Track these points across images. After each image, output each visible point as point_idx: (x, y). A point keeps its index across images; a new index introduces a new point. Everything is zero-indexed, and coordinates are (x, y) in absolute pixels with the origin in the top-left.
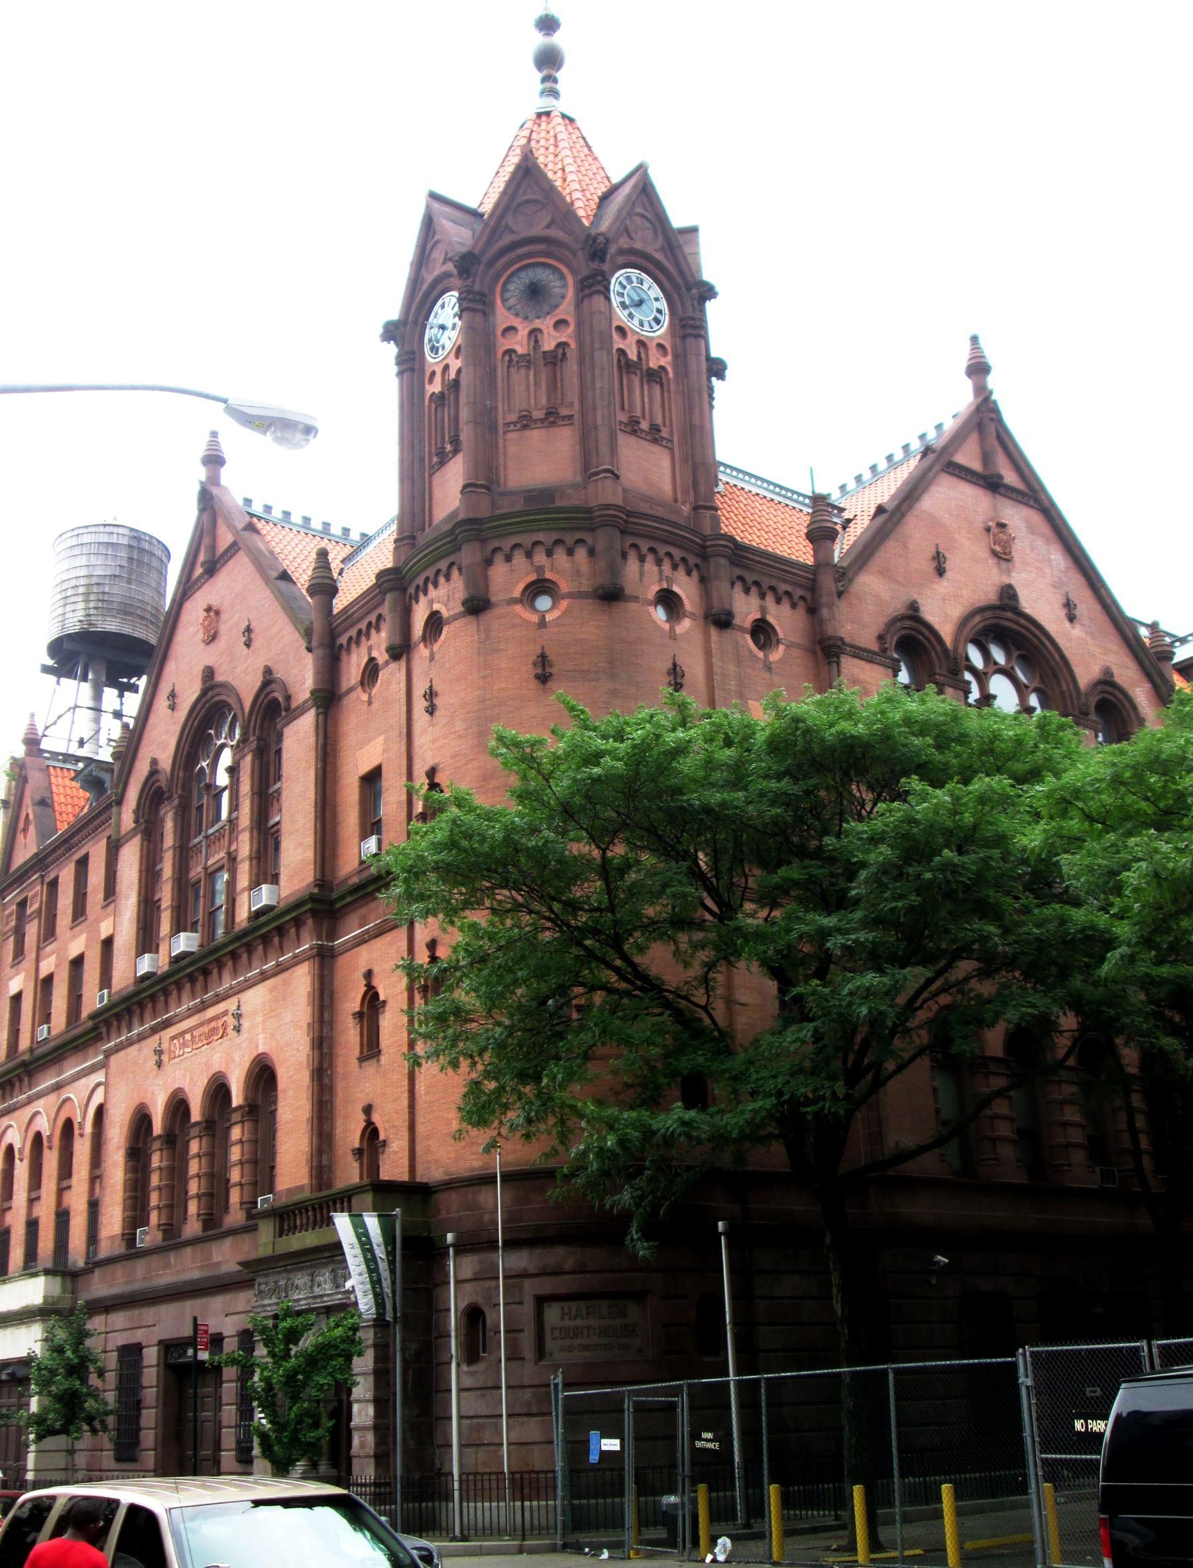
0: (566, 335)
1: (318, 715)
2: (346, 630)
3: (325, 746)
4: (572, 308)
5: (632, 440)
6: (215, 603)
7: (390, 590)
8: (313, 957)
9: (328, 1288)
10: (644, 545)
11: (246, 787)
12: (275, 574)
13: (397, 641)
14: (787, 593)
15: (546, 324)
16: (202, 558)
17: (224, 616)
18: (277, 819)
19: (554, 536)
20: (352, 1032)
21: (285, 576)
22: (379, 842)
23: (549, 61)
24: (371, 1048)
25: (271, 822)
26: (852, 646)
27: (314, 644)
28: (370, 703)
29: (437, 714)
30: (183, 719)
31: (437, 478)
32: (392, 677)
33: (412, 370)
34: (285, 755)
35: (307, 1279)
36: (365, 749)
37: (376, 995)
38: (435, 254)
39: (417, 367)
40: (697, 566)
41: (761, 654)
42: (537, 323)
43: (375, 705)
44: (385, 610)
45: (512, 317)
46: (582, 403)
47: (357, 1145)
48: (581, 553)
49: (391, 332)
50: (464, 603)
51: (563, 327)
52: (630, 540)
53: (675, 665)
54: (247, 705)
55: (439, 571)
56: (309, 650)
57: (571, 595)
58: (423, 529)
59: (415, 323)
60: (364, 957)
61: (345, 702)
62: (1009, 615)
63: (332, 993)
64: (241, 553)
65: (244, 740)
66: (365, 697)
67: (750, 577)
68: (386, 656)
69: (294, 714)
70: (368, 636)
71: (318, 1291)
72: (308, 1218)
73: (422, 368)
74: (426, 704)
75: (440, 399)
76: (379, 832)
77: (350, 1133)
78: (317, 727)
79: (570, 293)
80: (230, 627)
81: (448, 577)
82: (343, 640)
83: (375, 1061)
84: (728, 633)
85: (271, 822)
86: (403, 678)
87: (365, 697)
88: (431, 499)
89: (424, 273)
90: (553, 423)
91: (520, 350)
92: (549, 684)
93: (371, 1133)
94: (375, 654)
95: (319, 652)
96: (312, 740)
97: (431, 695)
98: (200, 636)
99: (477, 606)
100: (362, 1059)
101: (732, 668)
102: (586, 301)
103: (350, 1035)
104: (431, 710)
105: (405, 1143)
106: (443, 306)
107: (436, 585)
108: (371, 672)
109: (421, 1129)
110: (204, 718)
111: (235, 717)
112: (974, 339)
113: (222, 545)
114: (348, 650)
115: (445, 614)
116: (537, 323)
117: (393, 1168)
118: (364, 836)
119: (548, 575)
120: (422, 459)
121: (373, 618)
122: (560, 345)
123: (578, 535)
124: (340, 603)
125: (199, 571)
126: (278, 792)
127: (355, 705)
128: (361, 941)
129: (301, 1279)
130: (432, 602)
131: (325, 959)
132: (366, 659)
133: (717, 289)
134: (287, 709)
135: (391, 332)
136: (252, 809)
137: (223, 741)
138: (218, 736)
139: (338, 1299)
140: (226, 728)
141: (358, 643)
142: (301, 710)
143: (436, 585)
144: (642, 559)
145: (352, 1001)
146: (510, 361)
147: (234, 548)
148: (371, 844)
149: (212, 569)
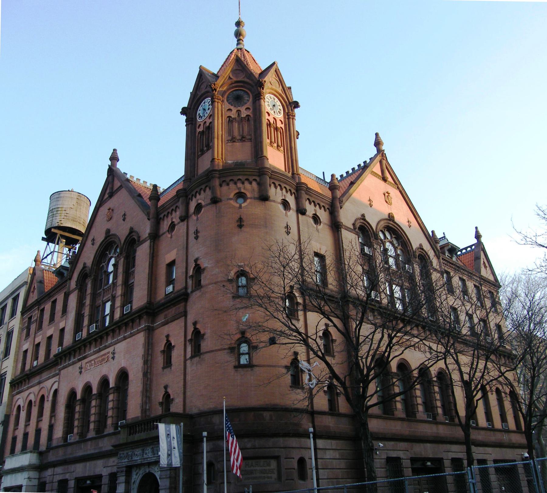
0: (249, 113)
1: (151, 242)
2: (163, 212)
3: (153, 253)
4: (252, 104)
5: (271, 148)
6: (112, 207)
7: (182, 196)
8: (145, 330)
9: (150, 455)
10: (277, 183)
11: (120, 270)
12: (136, 195)
13: (183, 214)
14: (323, 206)
15: (243, 109)
16: (108, 191)
17: (115, 211)
18: (133, 281)
19: (246, 177)
20: (160, 358)
21: (140, 195)
22: (174, 287)
23: (238, 35)
24: (168, 363)
25: (130, 283)
26: (345, 226)
27: (151, 217)
28: (171, 237)
29: (199, 239)
30: (97, 248)
31: (200, 159)
32: (181, 228)
33: (192, 124)
34: (137, 258)
35: (140, 452)
36: (169, 254)
37: (171, 344)
38: (202, 86)
39: (194, 123)
40: (294, 193)
41: (315, 226)
42: (239, 108)
43: (174, 238)
44: (179, 204)
45: (230, 106)
46: (255, 135)
47: (161, 401)
48: (254, 184)
49: (184, 111)
50: (211, 199)
51: (248, 110)
52: (273, 181)
53: (287, 225)
54: (122, 242)
55: (202, 189)
56: (149, 219)
57: (251, 198)
58: (194, 177)
59: (194, 108)
60: (166, 330)
61: (161, 238)
62: (391, 222)
63: (152, 344)
64: (123, 189)
65: (121, 253)
66: (169, 236)
67: (311, 199)
68: (179, 220)
69: (141, 243)
70: (171, 214)
71: (145, 456)
72: (142, 428)
73: (196, 124)
74: (194, 236)
75: (202, 133)
76: (173, 284)
77: (159, 396)
78: (150, 247)
79: (251, 100)
80: (118, 216)
81: (205, 191)
82: (162, 216)
83: (169, 369)
84: (304, 216)
85: (130, 283)
86: (186, 228)
87: (169, 236)
88: (197, 167)
89: (198, 92)
90: (244, 141)
91: (233, 117)
92: (243, 229)
93: (167, 396)
94: (174, 220)
95: (152, 220)
96: (148, 251)
97: (197, 232)
98: (106, 219)
99: (215, 201)
100: (164, 368)
101: (306, 229)
102: (257, 101)
103: (160, 360)
104: (197, 238)
105: (181, 399)
106: (205, 103)
107: (200, 194)
108: (172, 226)
109: (188, 394)
110: (105, 247)
111: (117, 246)
112: (377, 134)
113: (115, 187)
114: (163, 220)
115: (203, 203)
116: (239, 108)
117: (176, 407)
118: (168, 285)
119: (243, 191)
120: (195, 153)
121: (174, 207)
122: (247, 115)
123: (254, 178)
124: (160, 203)
125: (107, 196)
126: (133, 272)
127: (165, 241)
128: (166, 323)
129: (138, 451)
130: (198, 200)
131: (150, 331)
132: (170, 222)
133: (300, 104)
134: (139, 241)
135: (184, 111)
136: (123, 278)
137: (112, 255)
138: (110, 254)
139: (154, 459)
140: (113, 251)
141: (167, 217)
142: (145, 241)
143: (200, 194)
144: (276, 187)
145: (161, 346)
146: (229, 120)
147: (121, 187)
148: (170, 289)
149: (111, 195)
